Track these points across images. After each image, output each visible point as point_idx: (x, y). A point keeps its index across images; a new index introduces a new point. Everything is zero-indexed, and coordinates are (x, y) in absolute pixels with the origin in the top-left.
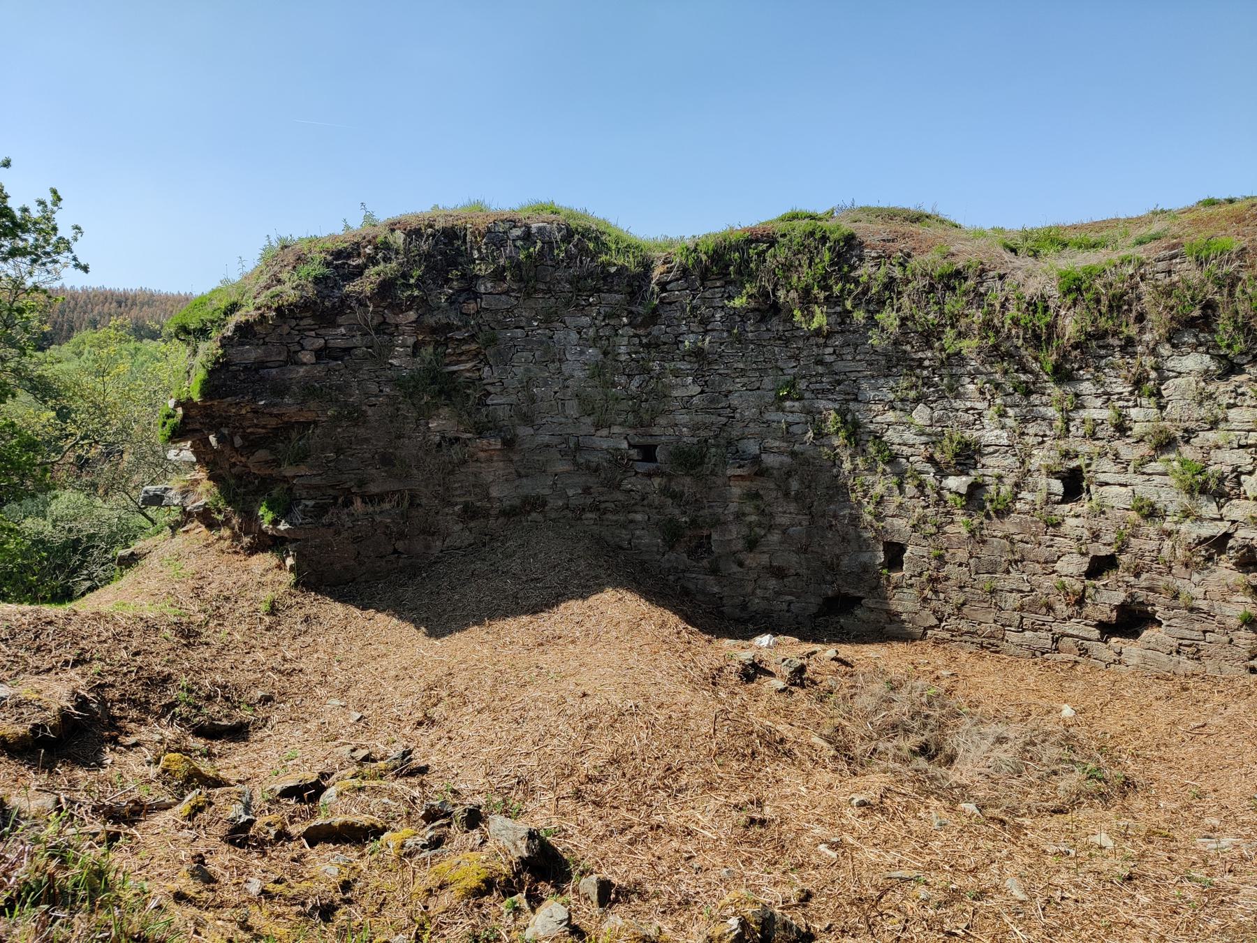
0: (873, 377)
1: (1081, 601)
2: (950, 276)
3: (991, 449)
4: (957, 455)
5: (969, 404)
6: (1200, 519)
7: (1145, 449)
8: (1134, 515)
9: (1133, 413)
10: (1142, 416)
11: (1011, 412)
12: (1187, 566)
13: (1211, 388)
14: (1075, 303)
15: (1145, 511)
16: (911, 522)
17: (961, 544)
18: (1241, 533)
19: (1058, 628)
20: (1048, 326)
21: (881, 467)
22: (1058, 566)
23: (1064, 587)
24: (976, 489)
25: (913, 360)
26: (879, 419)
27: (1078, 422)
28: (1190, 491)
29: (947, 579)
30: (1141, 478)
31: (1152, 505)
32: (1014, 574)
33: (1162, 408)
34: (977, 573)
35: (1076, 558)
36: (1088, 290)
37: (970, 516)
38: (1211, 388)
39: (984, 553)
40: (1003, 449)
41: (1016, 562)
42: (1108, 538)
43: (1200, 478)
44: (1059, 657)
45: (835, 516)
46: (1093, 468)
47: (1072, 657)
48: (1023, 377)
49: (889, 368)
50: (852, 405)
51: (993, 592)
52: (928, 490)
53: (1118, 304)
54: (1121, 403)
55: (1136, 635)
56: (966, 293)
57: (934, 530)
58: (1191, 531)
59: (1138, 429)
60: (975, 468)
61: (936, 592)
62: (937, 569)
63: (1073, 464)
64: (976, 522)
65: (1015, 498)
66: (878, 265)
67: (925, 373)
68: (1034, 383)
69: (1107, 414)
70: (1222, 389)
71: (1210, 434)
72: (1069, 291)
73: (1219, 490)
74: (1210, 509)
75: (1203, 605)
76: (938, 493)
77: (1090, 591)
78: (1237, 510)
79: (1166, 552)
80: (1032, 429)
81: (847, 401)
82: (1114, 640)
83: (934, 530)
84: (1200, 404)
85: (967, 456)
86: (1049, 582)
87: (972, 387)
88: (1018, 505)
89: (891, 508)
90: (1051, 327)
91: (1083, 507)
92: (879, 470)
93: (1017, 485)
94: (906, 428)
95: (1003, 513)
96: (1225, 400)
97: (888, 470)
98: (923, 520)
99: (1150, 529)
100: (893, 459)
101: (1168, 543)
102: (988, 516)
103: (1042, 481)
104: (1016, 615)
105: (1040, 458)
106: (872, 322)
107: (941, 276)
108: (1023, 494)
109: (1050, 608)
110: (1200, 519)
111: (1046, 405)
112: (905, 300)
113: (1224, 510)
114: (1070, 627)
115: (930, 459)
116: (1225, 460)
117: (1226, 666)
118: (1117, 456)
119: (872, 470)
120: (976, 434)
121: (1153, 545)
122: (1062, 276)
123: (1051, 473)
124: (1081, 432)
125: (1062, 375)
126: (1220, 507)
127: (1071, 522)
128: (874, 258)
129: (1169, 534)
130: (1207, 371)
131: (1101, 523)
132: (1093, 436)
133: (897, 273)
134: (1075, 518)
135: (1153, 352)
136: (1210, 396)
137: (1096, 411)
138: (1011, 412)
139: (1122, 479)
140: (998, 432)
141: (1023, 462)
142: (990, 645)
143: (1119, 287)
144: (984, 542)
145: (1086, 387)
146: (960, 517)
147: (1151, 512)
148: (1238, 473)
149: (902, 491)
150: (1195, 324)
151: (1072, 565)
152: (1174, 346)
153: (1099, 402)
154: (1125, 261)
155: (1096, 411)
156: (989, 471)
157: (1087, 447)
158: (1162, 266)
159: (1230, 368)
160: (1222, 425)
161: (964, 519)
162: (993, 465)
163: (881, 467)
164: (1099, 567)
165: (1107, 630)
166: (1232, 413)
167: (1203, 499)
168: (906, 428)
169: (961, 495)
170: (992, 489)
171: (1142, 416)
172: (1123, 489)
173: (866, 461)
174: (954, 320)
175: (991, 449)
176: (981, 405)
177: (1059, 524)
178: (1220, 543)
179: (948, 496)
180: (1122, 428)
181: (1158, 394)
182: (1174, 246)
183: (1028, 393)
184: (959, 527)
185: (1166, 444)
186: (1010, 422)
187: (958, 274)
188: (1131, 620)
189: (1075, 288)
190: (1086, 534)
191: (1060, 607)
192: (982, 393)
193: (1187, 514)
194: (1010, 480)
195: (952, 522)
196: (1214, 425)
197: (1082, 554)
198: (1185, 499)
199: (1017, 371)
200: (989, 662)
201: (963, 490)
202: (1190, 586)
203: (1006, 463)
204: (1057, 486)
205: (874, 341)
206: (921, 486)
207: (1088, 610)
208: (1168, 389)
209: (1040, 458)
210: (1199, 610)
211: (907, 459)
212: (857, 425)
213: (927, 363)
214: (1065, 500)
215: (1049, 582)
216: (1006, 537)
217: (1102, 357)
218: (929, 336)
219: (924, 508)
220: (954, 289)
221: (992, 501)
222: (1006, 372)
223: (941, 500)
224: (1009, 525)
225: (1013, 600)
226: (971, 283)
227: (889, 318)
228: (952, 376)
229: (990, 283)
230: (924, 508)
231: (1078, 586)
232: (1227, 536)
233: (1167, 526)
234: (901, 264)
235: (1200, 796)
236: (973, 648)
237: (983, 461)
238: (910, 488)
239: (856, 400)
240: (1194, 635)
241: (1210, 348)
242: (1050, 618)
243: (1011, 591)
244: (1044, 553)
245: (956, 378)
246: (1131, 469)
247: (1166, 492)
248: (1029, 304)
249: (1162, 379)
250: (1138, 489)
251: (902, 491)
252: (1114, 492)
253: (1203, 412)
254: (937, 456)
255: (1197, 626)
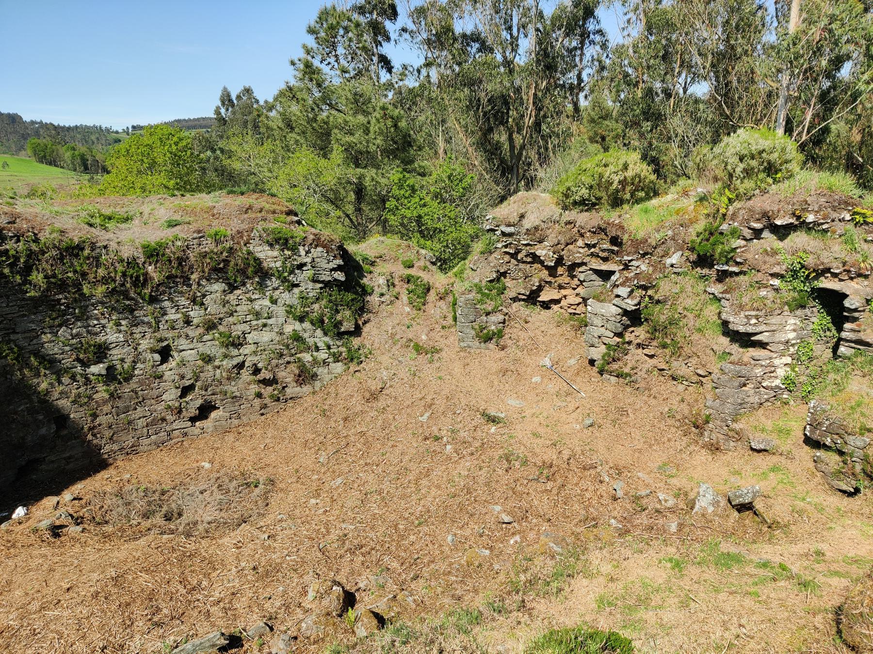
0: (24, 315)
1: (180, 412)
2: (73, 248)
3: (114, 345)
4: (95, 353)
5: (96, 322)
6: (232, 357)
7: (201, 330)
8: (200, 363)
9: (192, 314)
10: (196, 314)
11: (123, 322)
12: (228, 379)
13: (227, 298)
14: (157, 261)
15: (207, 359)
16: (70, 399)
17: (105, 402)
18: (249, 359)
19: (168, 429)
20: (143, 274)
21: (43, 371)
22: (164, 397)
23: (170, 407)
24: (111, 369)
25: (54, 300)
26: (35, 342)
27: (163, 322)
28: (227, 346)
29: (100, 425)
30: (200, 345)
31: (208, 356)
32: (139, 409)
33: (206, 309)
34: (118, 416)
35: (174, 391)
36: (163, 255)
37: (108, 385)
38: (227, 298)
39: (120, 404)
40: (121, 344)
41: (140, 402)
42: (188, 377)
43: (231, 339)
44: (172, 442)
45: (16, 413)
46: (175, 343)
47: (180, 439)
48: (128, 303)
49: (36, 308)
50: (12, 337)
51: (130, 423)
52: (78, 377)
53: (181, 261)
54: (185, 310)
55: (206, 418)
56: (88, 258)
57: (86, 400)
58: (228, 364)
59: (195, 321)
60: (106, 358)
61: (94, 435)
62: (93, 421)
63: (165, 344)
64: (112, 388)
65: (134, 369)
66: (18, 241)
67: (63, 307)
68: (135, 305)
69: (179, 316)
70: (231, 297)
71: (230, 319)
72: (152, 256)
73: (237, 343)
74: (235, 352)
75: (238, 394)
76: (86, 378)
77: (183, 404)
78: (247, 350)
79: (218, 376)
80: (140, 329)
81: (8, 334)
82: (197, 424)
83: (86, 400)
84: (224, 306)
85: (101, 352)
86: (160, 407)
87: (96, 312)
88: (136, 372)
89: (56, 395)
90: (146, 274)
91: (172, 363)
92: (42, 374)
93: (134, 362)
94: (57, 343)
95: (127, 380)
96: (235, 303)
97: (47, 372)
98: (79, 396)
99: (210, 367)
100: (51, 363)
101: (218, 371)
102: (120, 383)
103: (149, 356)
104: (145, 430)
105: (145, 344)
106: (25, 282)
107: (67, 249)
108: (139, 365)
109: (163, 420)
110: (232, 357)
111: (144, 316)
112: (44, 265)
113: (241, 351)
114: (175, 426)
115: (78, 360)
116: (238, 330)
117: (252, 417)
118: (187, 336)
119: (38, 375)
120: (103, 339)
121: (211, 374)
122: (144, 247)
123: (153, 351)
124: (166, 327)
125: (153, 300)
126: (239, 350)
127: (167, 373)
128: (11, 237)
129: (219, 367)
130: (224, 291)
131: (183, 370)
132: (173, 328)
133: (34, 247)
134: (169, 370)
135: (199, 284)
136: (228, 302)
137: (172, 315)
138: (123, 322)
139: (191, 346)
140: (117, 335)
141: (136, 349)
142: (133, 451)
143: (180, 254)
144: (119, 398)
145: (167, 304)
146: (101, 387)
147: (208, 359)
148: (244, 333)
149: (60, 383)
150: (219, 271)
151: (171, 396)
152: (208, 280)
153: (174, 311)
154: (177, 239)
155: (172, 315)
156: (115, 358)
157: (170, 334)
158: (195, 241)
159: (232, 288)
160: (235, 314)
161: (104, 388)
162: (116, 354)
163: (43, 371)
164: (186, 391)
165: (193, 420)
166: (238, 308)
167: (231, 348)
168: (57, 343)
169: (102, 376)
170: (119, 367)
171: (196, 314)
172: (193, 351)
173: (31, 370)
174: (84, 275)
175: (114, 345)
176: (103, 322)
177: (161, 377)
178: (241, 366)
179: (92, 377)
180: (188, 322)
181: (202, 304)
182: (199, 232)
183: (132, 311)
184: (102, 392)
185: (210, 326)
186: (122, 328)
187: (80, 248)
188: (205, 411)
189: (153, 253)
190: (177, 377)
191: (169, 418)
192: (103, 314)
193: (226, 356)
194: (129, 360)
195: (97, 392)
196: (231, 315)
197: (177, 388)
198: (224, 350)
199: (123, 299)
200: (136, 461)
201: (104, 372)
202: (232, 388)
203: (125, 351)
204: (157, 357)
205: (32, 294)
206: (73, 378)
207: (184, 413)
208: (207, 301)
209: (145, 344)
210: (236, 397)
211: (60, 362)
212: (20, 348)
213: (63, 301)
214: (162, 364)
215: (160, 407)
216: (132, 391)
217: (171, 288)
218: (62, 286)
219: (77, 389)
220: (77, 256)
221: (120, 375)
222: (118, 301)
223: (88, 381)
224: (133, 384)
225: (141, 423)
226: (86, 252)
227: (37, 277)
228: (81, 307)
229: (98, 250)
230: (77, 389)
231: (177, 404)
232: (244, 362)
233: (217, 363)
234: (34, 241)
235: (297, 471)
236: (122, 457)
237: (109, 353)
238: (66, 380)
239: (14, 332)
240: (236, 408)
241: (226, 280)
242: (164, 424)
243: (140, 418)
244: (156, 393)
245: (84, 309)
246: (195, 341)
247: (212, 348)
248: (128, 263)
249: (204, 296)
250: (201, 350)
251: (60, 383)
252: (187, 352)
253: (225, 309)
254: (81, 356)
255: (237, 404)
